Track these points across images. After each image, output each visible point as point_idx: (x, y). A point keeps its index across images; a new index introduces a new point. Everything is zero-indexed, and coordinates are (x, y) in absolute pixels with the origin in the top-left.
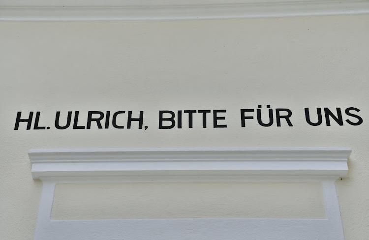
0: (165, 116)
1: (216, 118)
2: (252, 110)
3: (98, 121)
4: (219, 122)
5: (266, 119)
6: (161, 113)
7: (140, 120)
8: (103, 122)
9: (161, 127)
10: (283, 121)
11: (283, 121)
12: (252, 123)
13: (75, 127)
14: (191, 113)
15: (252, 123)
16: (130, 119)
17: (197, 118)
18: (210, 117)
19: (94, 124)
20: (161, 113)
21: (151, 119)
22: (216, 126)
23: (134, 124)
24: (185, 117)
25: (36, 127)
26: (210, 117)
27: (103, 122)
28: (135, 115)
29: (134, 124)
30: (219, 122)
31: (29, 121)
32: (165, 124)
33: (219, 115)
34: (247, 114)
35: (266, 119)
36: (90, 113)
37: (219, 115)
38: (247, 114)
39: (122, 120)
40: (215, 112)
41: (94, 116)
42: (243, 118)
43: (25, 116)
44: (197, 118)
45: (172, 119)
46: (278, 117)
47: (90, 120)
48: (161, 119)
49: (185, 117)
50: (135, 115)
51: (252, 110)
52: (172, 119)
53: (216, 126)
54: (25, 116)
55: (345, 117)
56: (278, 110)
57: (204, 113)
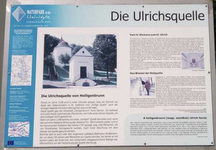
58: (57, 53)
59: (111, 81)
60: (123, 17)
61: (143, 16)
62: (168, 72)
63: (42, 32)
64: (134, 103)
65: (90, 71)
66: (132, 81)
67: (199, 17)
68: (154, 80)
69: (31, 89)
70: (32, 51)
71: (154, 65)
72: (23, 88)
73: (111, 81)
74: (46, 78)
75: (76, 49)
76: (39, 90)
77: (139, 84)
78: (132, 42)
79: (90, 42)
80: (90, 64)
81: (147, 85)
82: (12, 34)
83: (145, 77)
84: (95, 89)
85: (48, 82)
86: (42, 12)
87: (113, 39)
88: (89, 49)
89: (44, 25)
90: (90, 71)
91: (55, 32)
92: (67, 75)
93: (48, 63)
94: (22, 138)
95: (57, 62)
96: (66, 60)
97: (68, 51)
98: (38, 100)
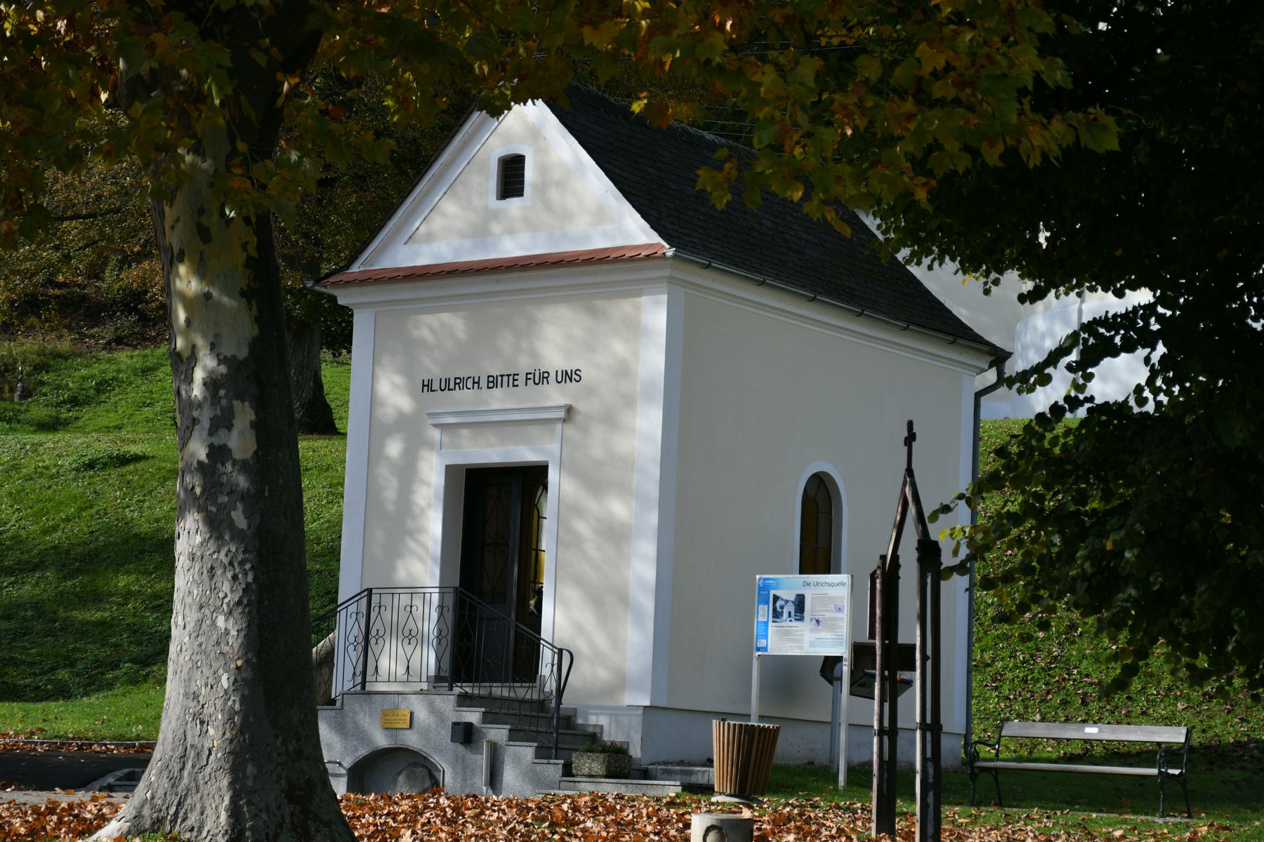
0: (491, 379)
1: (514, 380)
2: (531, 373)
3: (459, 384)
4: (516, 383)
5: (537, 381)
6: (489, 377)
7: (478, 383)
8: (461, 385)
9: (488, 388)
10: (545, 380)
11: (545, 380)
13: (449, 390)
14: (502, 376)
16: (474, 383)
17: (505, 378)
18: (511, 378)
19: (457, 386)
20: (489, 377)
21: (483, 383)
22: (514, 386)
23: (476, 385)
24: (499, 378)
25: (432, 391)
26: (511, 378)
27: (461, 385)
28: (476, 380)
29: (476, 385)
30: (516, 383)
31: (428, 386)
32: (491, 385)
33: (516, 377)
34: (529, 376)
35: (537, 381)
36: (456, 379)
37: (516, 377)
38: (529, 376)
40: (514, 375)
41: (458, 381)
42: (527, 379)
43: (426, 383)
44: (505, 378)
45: (493, 382)
46: (543, 378)
47: (455, 384)
48: (489, 382)
49: (499, 378)
50: (476, 380)
51: (531, 373)
52: (493, 382)
53: (514, 386)
54: (426, 383)
55: (574, 376)
56: (544, 372)
57: (509, 375)
58: (778, 604)
59: (801, 619)
60: (809, 584)
62: (828, 615)
63: (772, 592)
64: (812, 631)
65: (793, 614)
66: (811, 619)
67: (844, 584)
68: (821, 619)
69: (767, 623)
70: (767, 603)
71: (821, 611)
72: (764, 622)
73: (801, 619)
74: (773, 617)
75: (787, 602)
76: (771, 624)
77: (814, 621)
78: (813, 598)
79: (792, 598)
81: (818, 621)
82: (759, 594)
83: (817, 617)
85: (775, 620)
86: (772, 582)
87: (803, 596)
88: (793, 602)
89: (774, 589)
90: (793, 614)
91: (778, 593)
92: (782, 616)
93: (775, 609)
94: (763, 648)
95: (779, 609)
96: (782, 607)
97: (783, 603)
98: (770, 628)
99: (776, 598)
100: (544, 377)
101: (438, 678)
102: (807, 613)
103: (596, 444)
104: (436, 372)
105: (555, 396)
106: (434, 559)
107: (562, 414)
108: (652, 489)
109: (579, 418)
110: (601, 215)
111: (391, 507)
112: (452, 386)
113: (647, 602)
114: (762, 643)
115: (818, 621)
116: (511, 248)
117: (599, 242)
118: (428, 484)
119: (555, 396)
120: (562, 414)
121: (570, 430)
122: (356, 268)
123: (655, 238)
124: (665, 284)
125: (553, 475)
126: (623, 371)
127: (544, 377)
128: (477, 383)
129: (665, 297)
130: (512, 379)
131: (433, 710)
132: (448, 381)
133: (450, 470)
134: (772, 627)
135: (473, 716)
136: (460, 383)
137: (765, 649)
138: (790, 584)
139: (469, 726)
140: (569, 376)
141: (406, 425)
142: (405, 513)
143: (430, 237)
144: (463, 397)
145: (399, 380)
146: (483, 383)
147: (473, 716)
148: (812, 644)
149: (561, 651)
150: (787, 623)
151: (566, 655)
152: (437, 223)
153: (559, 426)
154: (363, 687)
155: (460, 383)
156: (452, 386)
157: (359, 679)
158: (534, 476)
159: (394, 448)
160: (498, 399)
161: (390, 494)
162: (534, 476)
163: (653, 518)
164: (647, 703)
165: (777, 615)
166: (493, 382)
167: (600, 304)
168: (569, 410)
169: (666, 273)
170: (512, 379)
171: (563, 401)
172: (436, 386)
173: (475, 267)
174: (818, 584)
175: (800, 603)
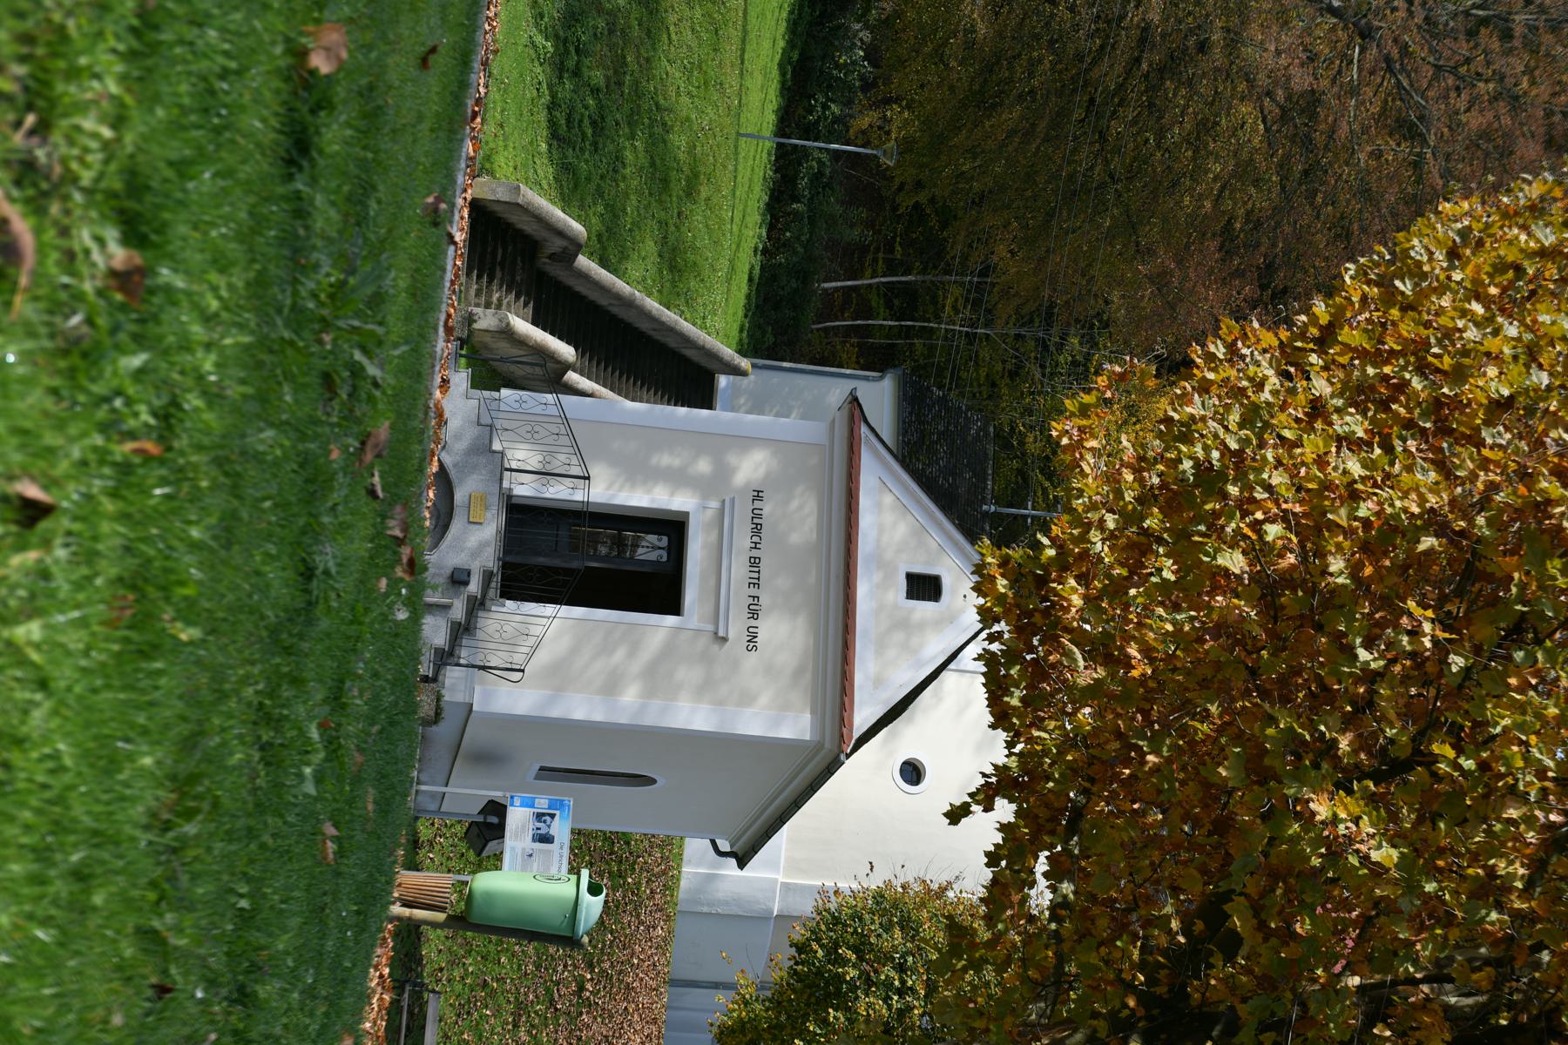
12: (751, 601)
15: (751, 601)
17: (756, 575)
21: (755, 553)
39: (756, 539)
44: (756, 575)
58: (548, 818)
59: (534, 840)
61: (561, 856)
62: (535, 865)
63: (557, 812)
64: (524, 849)
69: (532, 806)
73: (534, 840)
75: (549, 826)
76: (532, 810)
79: (552, 832)
80: (542, 832)
81: (531, 855)
84: (531, 833)
91: (557, 818)
93: (544, 814)
96: (545, 822)
99: (552, 816)
100: (754, 614)
101: (510, 497)
102: (538, 845)
103: (690, 674)
104: (767, 508)
105: (736, 629)
106: (613, 496)
107: (721, 633)
108: (649, 720)
109: (716, 647)
110: (878, 682)
111: (655, 460)
112: (755, 521)
113: (556, 712)
114: (517, 801)
115: (531, 855)
116: (862, 590)
117: (859, 678)
118: (672, 494)
119: (736, 629)
120: (721, 633)
121: (704, 641)
122: (864, 429)
123: (856, 735)
124: (817, 738)
125: (670, 620)
126: (747, 699)
127: (754, 614)
128: (755, 546)
129: (807, 737)
130: (755, 583)
131: (483, 545)
132: (760, 516)
133: (687, 514)
134: (528, 812)
135: (474, 587)
136: (757, 529)
137: (512, 805)
138: (561, 829)
139: (466, 583)
140: (753, 638)
141: (723, 473)
142: (651, 475)
143: (879, 506)
144: (743, 540)
145: (761, 471)
146: (755, 553)
147: (474, 587)
148: (513, 849)
149: (523, 671)
150: (532, 825)
151: (518, 675)
152: (888, 518)
153: (710, 627)
154: (507, 470)
155: (757, 529)
156: (755, 521)
157: (514, 467)
158: (672, 605)
159: (703, 466)
160: (738, 569)
161: (666, 460)
162: (672, 605)
163: (623, 720)
164: (474, 708)
165: (539, 817)
166: (754, 562)
167: (808, 677)
168: (725, 639)
169: (827, 745)
170: (755, 583)
171: (731, 636)
172: (757, 504)
173: (852, 546)
174: (561, 856)
175: (546, 839)
